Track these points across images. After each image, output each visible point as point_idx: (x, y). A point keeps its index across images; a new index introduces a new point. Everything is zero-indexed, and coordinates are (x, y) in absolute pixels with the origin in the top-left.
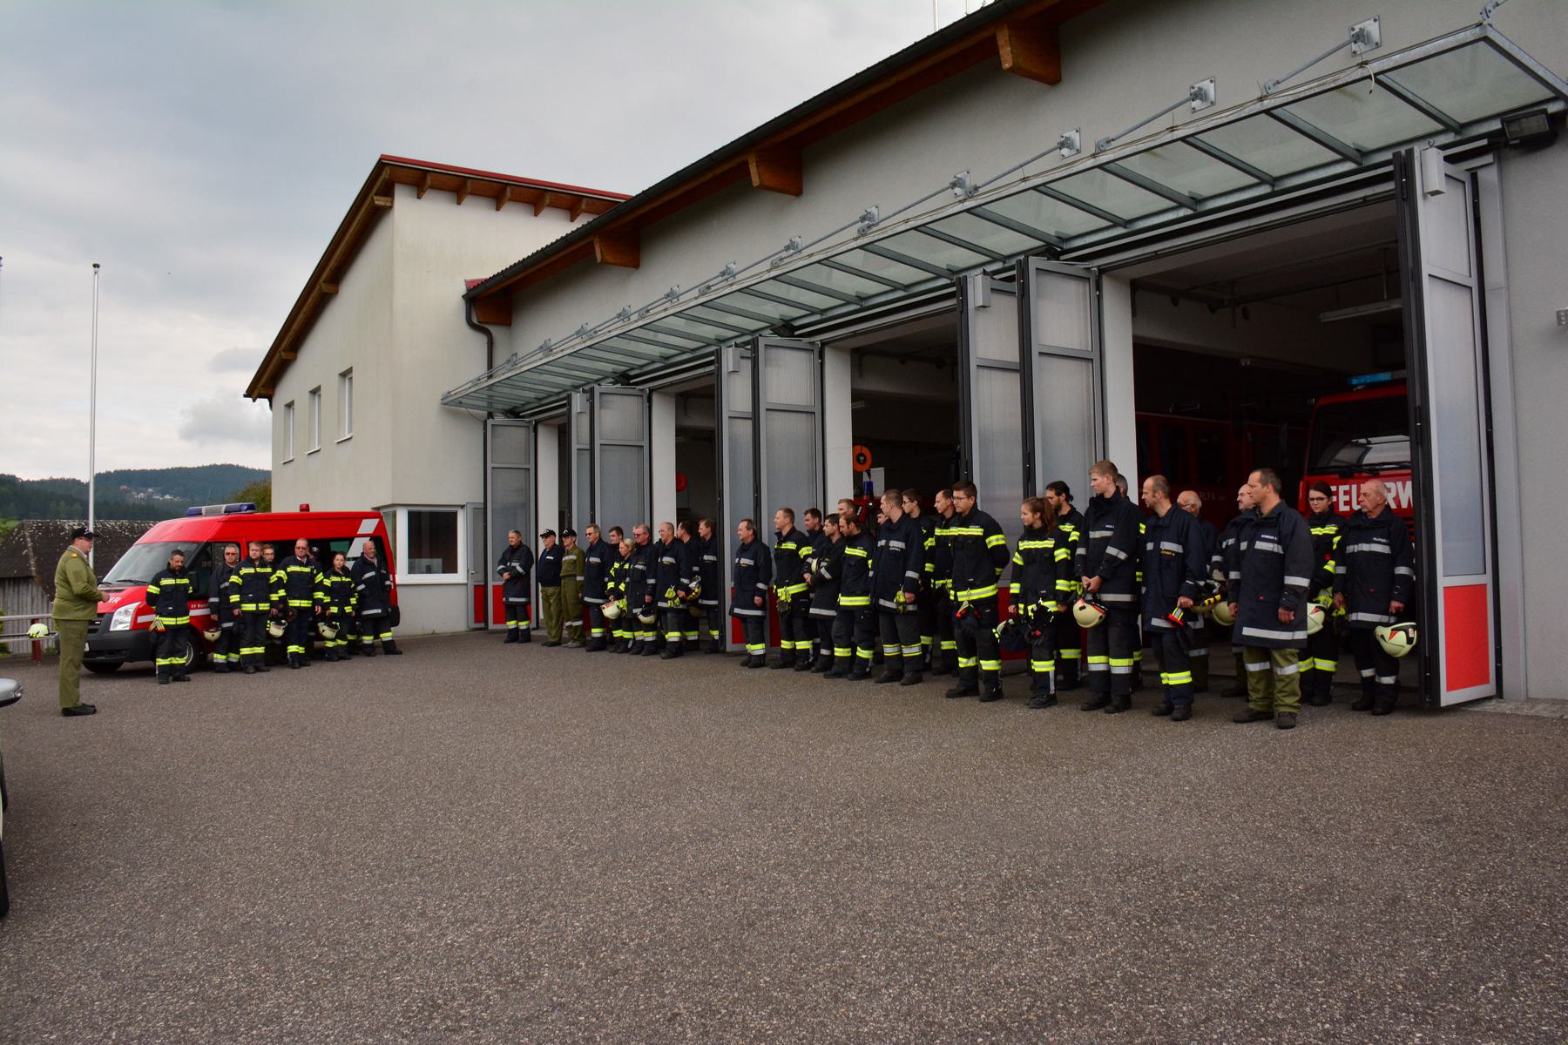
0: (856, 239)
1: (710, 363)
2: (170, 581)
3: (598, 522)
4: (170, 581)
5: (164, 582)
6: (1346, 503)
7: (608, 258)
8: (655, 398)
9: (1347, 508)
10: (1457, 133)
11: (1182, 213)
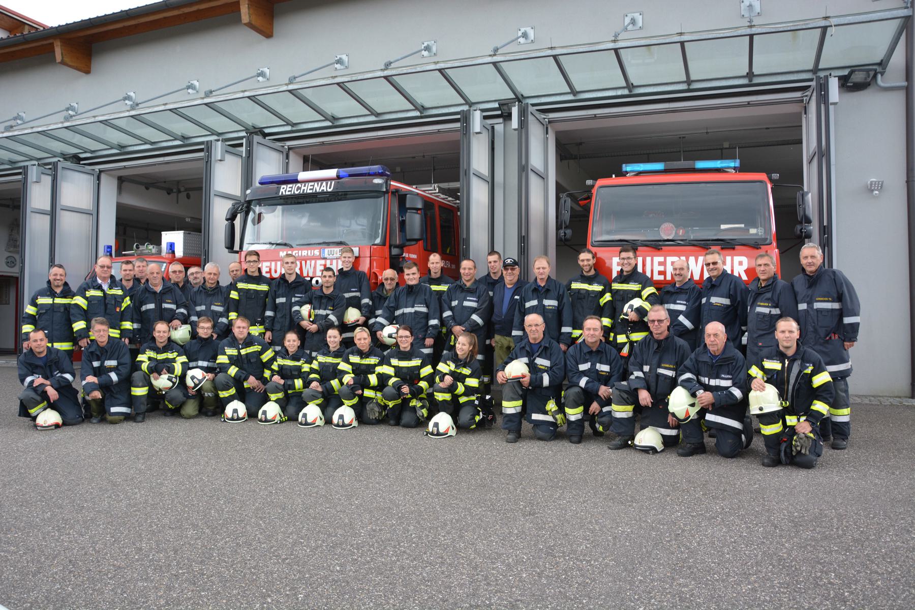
0: (203, 98)
1: (201, 150)
2: (48, 301)
3: (498, 247)
4: (48, 301)
5: (41, 301)
6: (660, 273)
7: (67, 60)
8: (103, 176)
9: (661, 278)
10: (574, 95)
11: (373, 118)
